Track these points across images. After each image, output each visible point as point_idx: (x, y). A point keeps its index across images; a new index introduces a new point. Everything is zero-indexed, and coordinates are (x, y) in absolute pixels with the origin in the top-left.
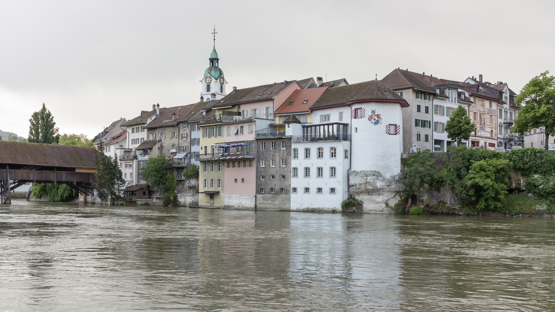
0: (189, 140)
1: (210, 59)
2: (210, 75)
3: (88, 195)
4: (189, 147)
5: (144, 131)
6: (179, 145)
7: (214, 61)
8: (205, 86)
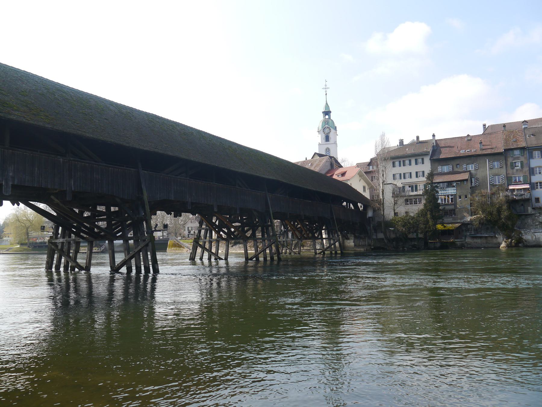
0: (526, 169)
1: (323, 112)
2: (328, 126)
3: (348, 239)
4: (529, 177)
5: (423, 163)
6: (508, 176)
7: (327, 113)
8: (324, 136)
